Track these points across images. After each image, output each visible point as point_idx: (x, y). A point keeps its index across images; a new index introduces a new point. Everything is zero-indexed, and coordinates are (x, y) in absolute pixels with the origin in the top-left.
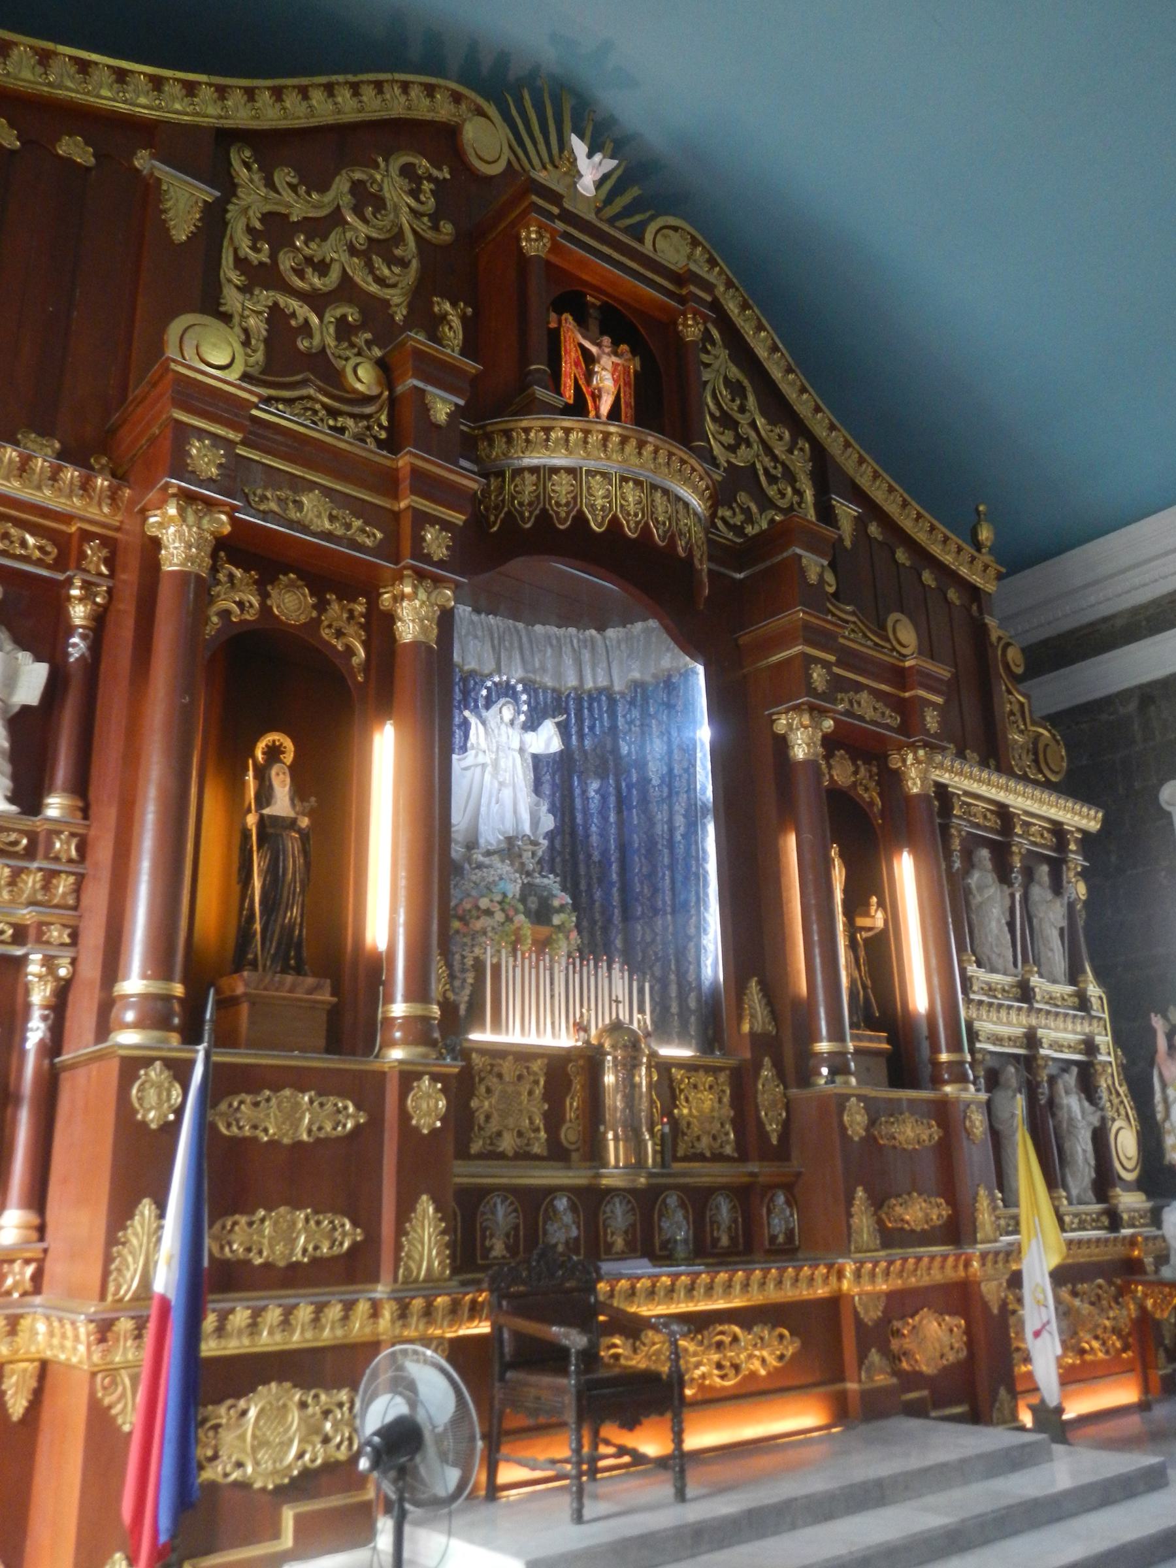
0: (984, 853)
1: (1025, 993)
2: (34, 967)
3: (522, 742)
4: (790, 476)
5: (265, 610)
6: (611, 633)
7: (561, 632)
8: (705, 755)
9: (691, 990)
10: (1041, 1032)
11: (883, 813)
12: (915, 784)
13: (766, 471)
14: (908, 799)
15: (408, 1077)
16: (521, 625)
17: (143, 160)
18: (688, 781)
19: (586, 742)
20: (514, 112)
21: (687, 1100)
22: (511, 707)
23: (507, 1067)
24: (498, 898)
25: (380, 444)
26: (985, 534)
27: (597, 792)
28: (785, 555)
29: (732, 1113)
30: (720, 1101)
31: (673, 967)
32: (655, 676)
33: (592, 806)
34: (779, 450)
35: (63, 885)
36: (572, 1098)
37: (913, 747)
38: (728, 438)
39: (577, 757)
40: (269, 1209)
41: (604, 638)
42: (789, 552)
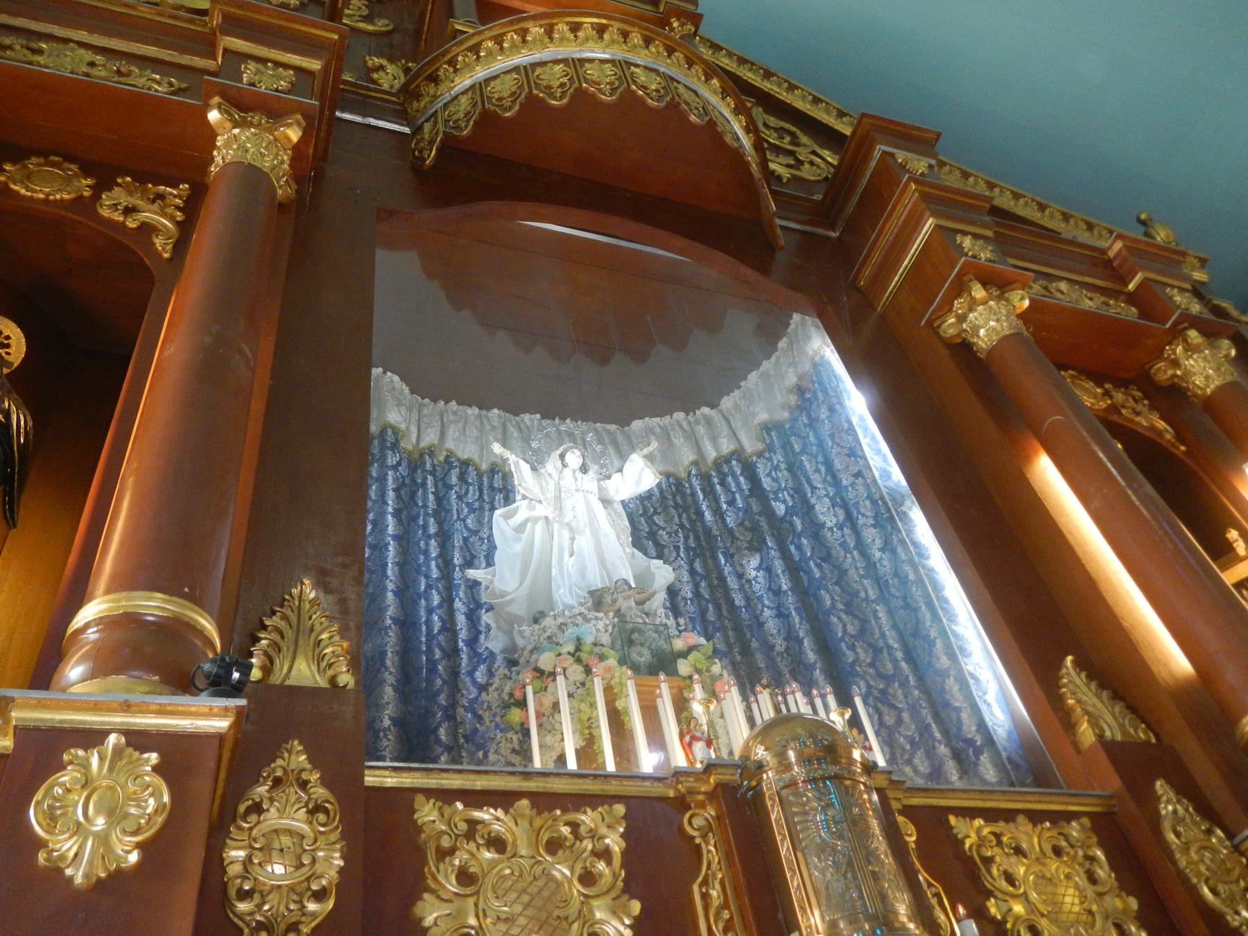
3: (600, 489)
6: (727, 403)
7: (667, 419)
8: (873, 438)
9: (978, 752)
11: (1180, 437)
12: (1207, 377)
14: (1209, 404)
16: (613, 427)
18: (867, 486)
19: (728, 519)
21: (1010, 879)
22: (577, 452)
24: (571, 648)
27: (757, 569)
28: (873, 164)
29: (1133, 903)
30: (1092, 879)
31: (938, 735)
32: (784, 407)
33: (756, 587)
36: (705, 883)
37: (1176, 333)
39: (715, 532)
41: (721, 412)
42: (877, 154)
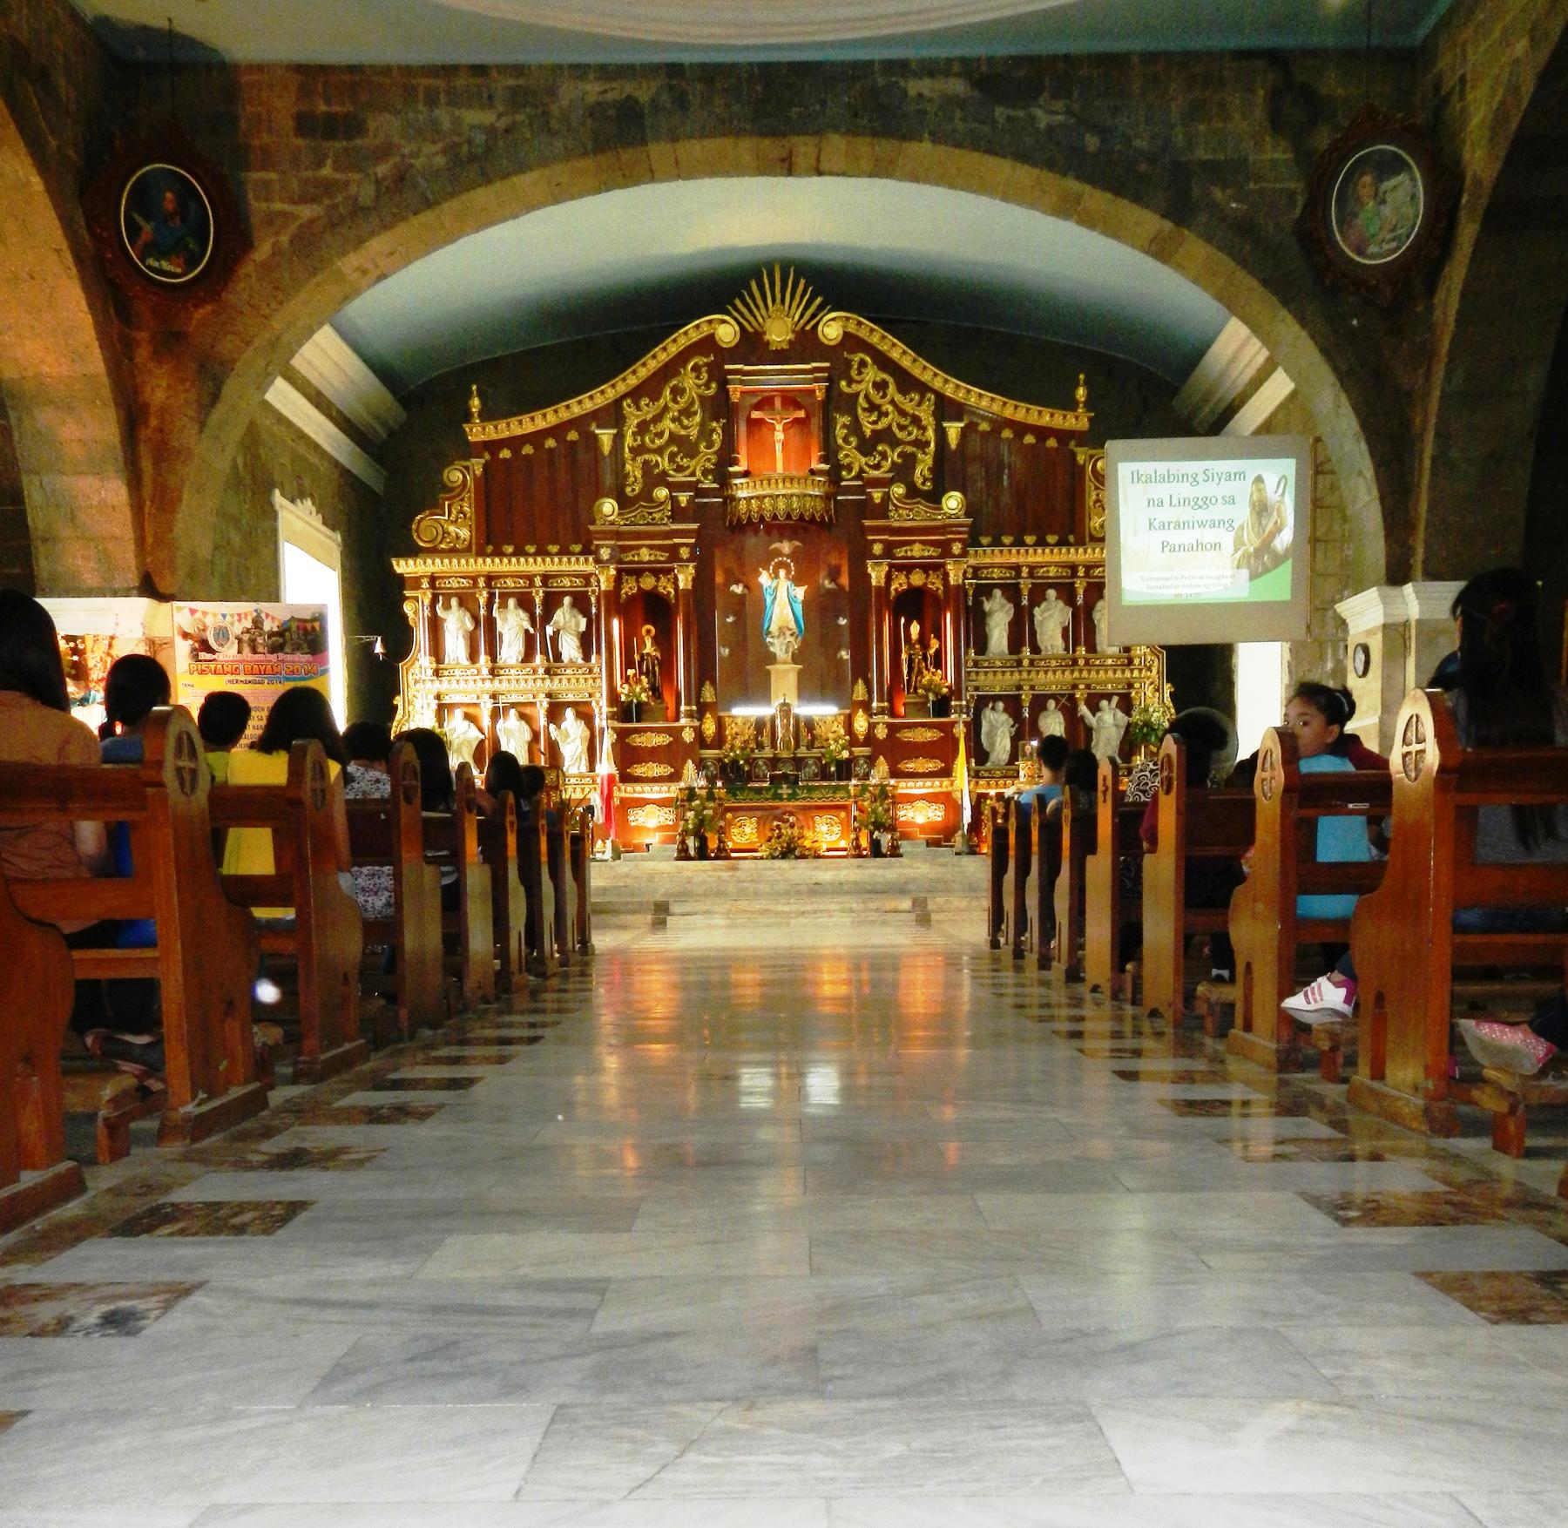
0: (1051, 593)
1: (1075, 662)
2: (594, 704)
4: (916, 421)
5: (639, 587)
10: (1077, 682)
13: (898, 425)
15: (682, 728)
17: (593, 427)
20: (749, 301)
23: (739, 721)
25: (669, 517)
26: (1081, 393)
34: (909, 407)
35: (598, 681)
38: (874, 418)
40: (646, 762)
